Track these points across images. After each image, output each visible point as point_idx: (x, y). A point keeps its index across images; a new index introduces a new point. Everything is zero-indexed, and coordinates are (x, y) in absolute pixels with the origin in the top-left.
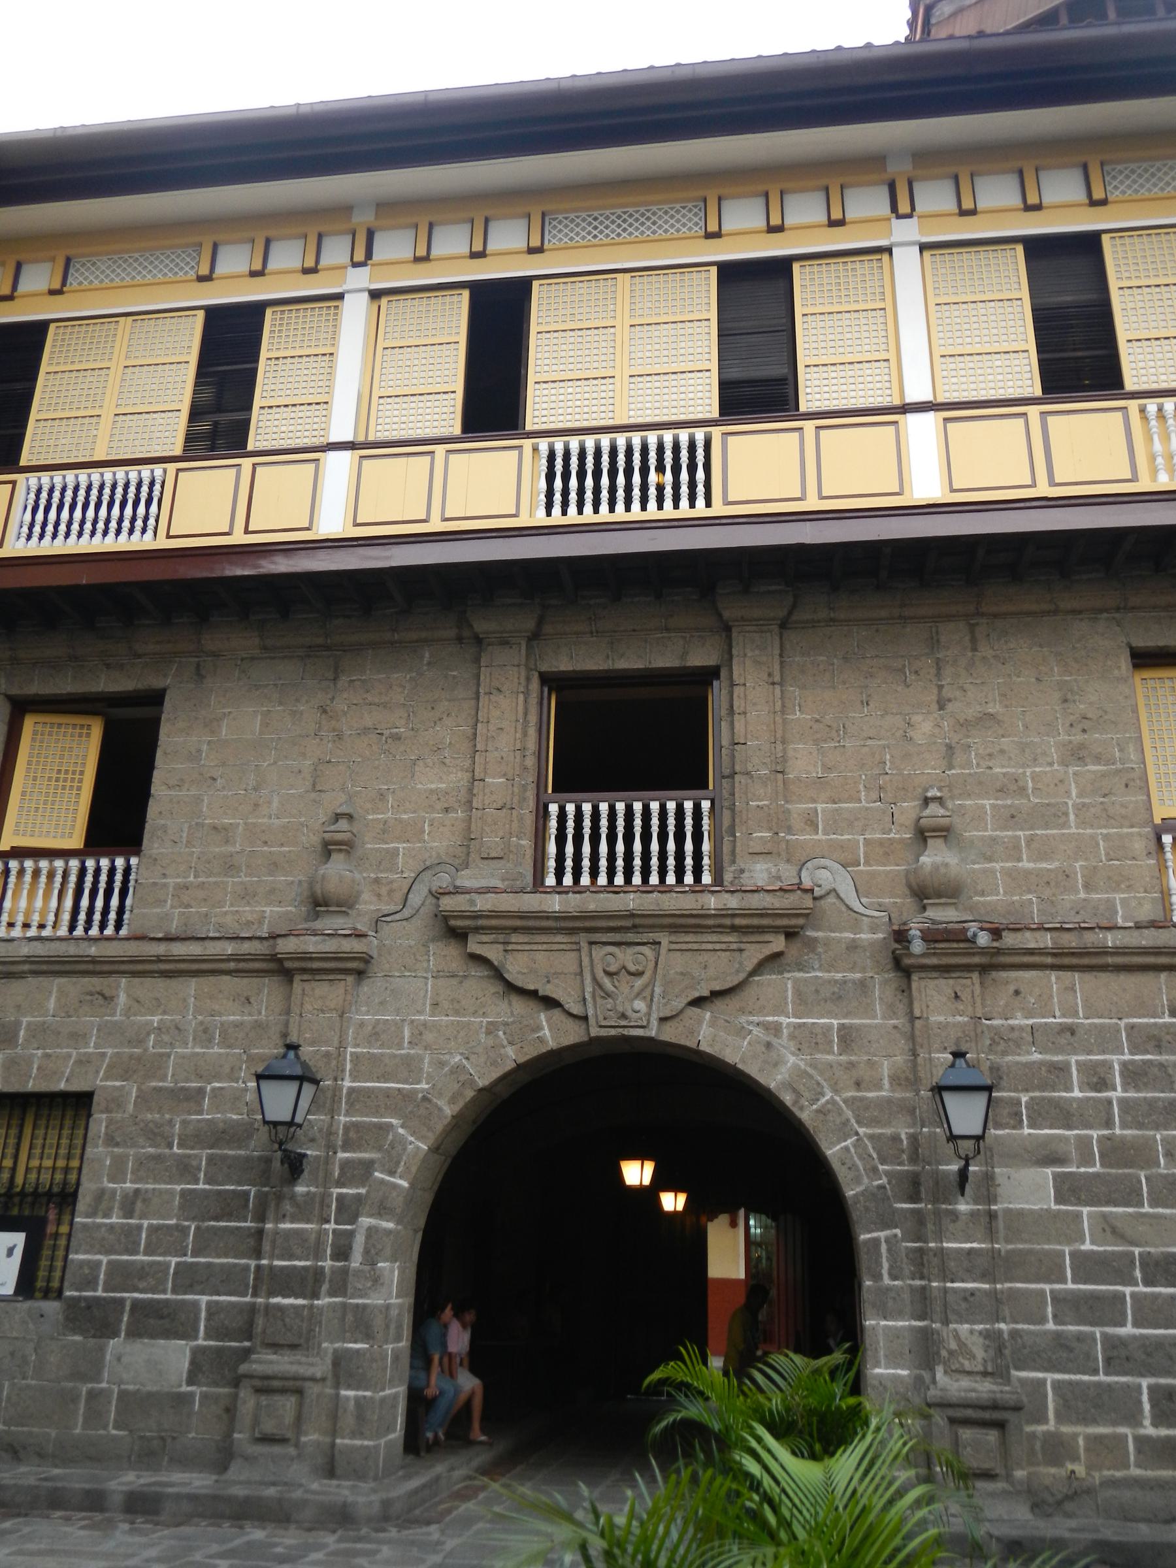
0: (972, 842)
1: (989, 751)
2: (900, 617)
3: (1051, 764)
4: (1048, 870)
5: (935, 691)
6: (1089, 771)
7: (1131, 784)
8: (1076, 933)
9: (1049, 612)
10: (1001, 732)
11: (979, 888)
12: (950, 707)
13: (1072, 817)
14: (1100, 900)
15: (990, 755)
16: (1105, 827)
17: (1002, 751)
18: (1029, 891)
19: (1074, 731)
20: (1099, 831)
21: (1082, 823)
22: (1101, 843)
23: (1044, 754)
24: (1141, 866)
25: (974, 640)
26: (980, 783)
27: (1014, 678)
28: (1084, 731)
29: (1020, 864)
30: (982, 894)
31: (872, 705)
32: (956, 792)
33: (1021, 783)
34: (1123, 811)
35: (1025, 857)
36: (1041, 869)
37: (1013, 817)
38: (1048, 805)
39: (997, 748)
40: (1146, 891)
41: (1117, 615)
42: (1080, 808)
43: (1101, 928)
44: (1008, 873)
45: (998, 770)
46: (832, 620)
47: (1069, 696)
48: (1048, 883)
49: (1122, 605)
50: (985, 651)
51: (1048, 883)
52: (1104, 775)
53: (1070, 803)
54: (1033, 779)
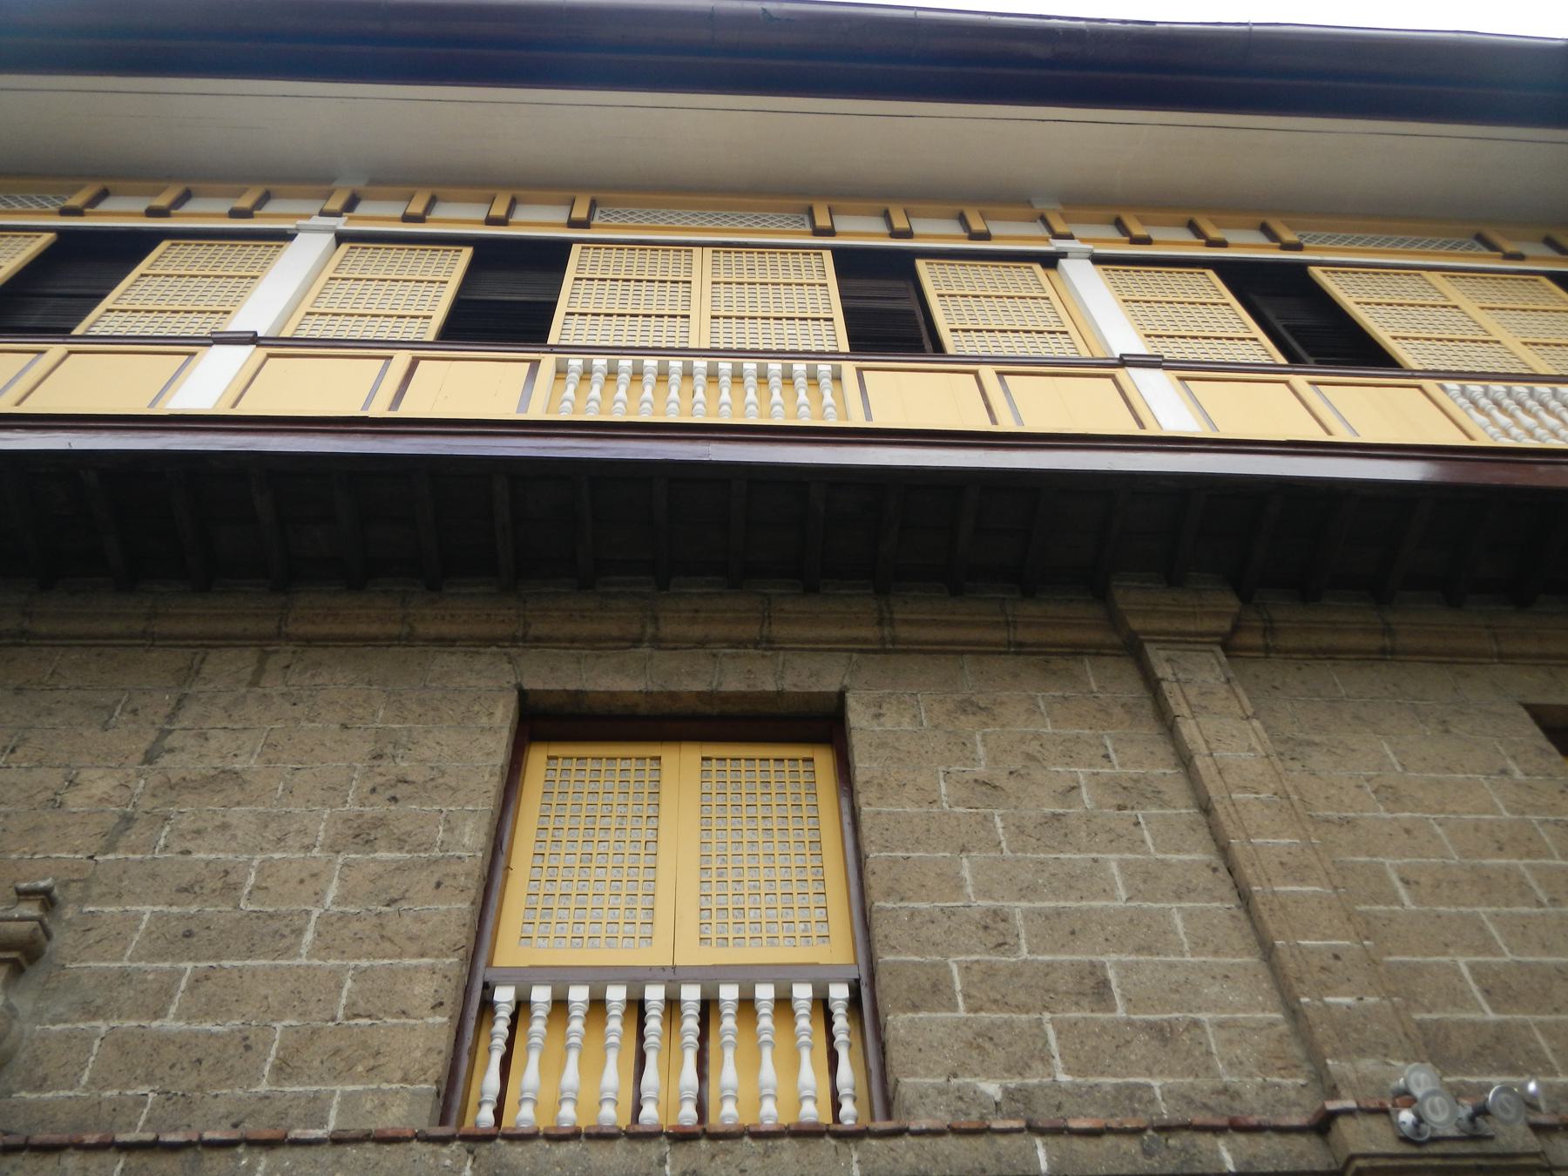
0: (77, 979)
1: (200, 824)
2: (144, 634)
3: (308, 848)
4: (211, 1035)
5: (152, 735)
6: (374, 860)
7: (448, 882)
8: (189, 1155)
9: (398, 638)
10: (238, 797)
11: (40, 1071)
12: (165, 760)
13: (309, 937)
14: (297, 1096)
15: (198, 832)
16: (369, 955)
17: (225, 826)
18: (149, 1079)
19: (374, 798)
20: (352, 963)
21: (325, 947)
22: (349, 984)
23: (303, 832)
24: (413, 1028)
25: (259, 672)
26: (154, 876)
27: (304, 723)
28: (394, 799)
29: (156, 1024)
30: (39, 1088)
31: (19, 753)
32: (95, 891)
33: (233, 878)
34: (415, 928)
35: (173, 1009)
36: (196, 1035)
37: (188, 934)
38: (271, 916)
39: (218, 820)
40: (405, 1079)
41: (513, 651)
42: (325, 920)
43: (252, 1143)
44: (118, 1042)
45: (202, 855)
46: (23, 633)
47: (389, 750)
48: (199, 1061)
49: (520, 633)
50: (273, 684)
51: (199, 1061)
52: (400, 868)
53: (316, 912)
54: (260, 871)
